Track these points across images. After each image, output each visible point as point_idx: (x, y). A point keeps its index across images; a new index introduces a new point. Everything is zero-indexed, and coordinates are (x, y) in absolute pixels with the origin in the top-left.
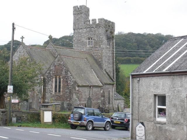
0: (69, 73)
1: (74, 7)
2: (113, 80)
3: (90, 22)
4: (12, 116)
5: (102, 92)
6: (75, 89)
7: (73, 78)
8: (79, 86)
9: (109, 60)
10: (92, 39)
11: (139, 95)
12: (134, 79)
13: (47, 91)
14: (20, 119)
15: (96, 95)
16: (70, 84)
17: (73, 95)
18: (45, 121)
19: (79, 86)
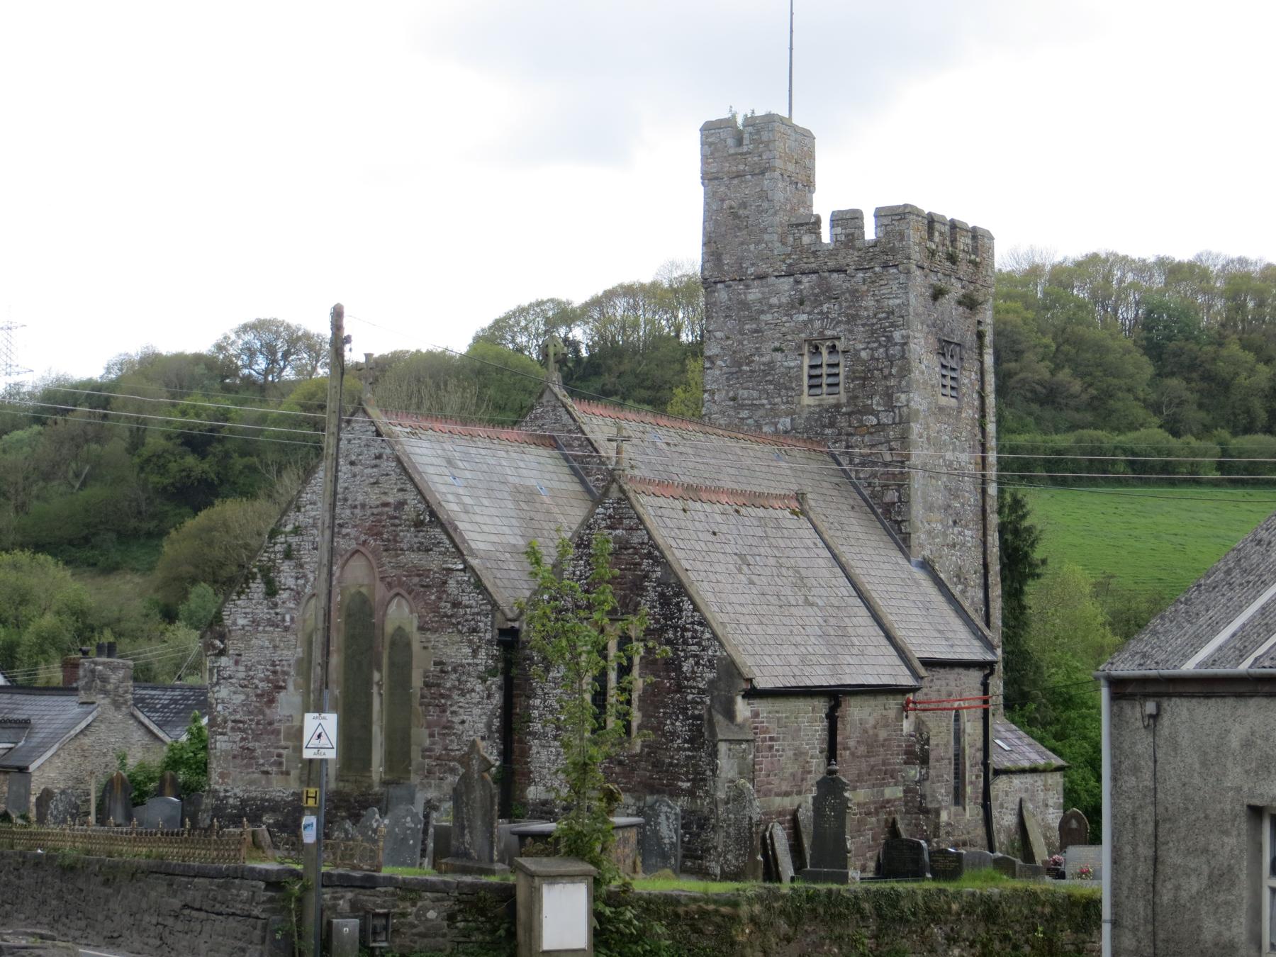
0: (687, 606)
1: (709, 129)
2: (987, 632)
3: (818, 235)
4: (334, 908)
5: (907, 726)
6: (730, 714)
7: (715, 637)
8: (753, 694)
9: (954, 493)
10: (833, 350)
11: (1155, 804)
12: (1124, 704)
13: (537, 726)
14: (386, 928)
15: (869, 754)
16: (691, 683)
17: (714, 754)
18: (547, 945)
19: (753, 694)
